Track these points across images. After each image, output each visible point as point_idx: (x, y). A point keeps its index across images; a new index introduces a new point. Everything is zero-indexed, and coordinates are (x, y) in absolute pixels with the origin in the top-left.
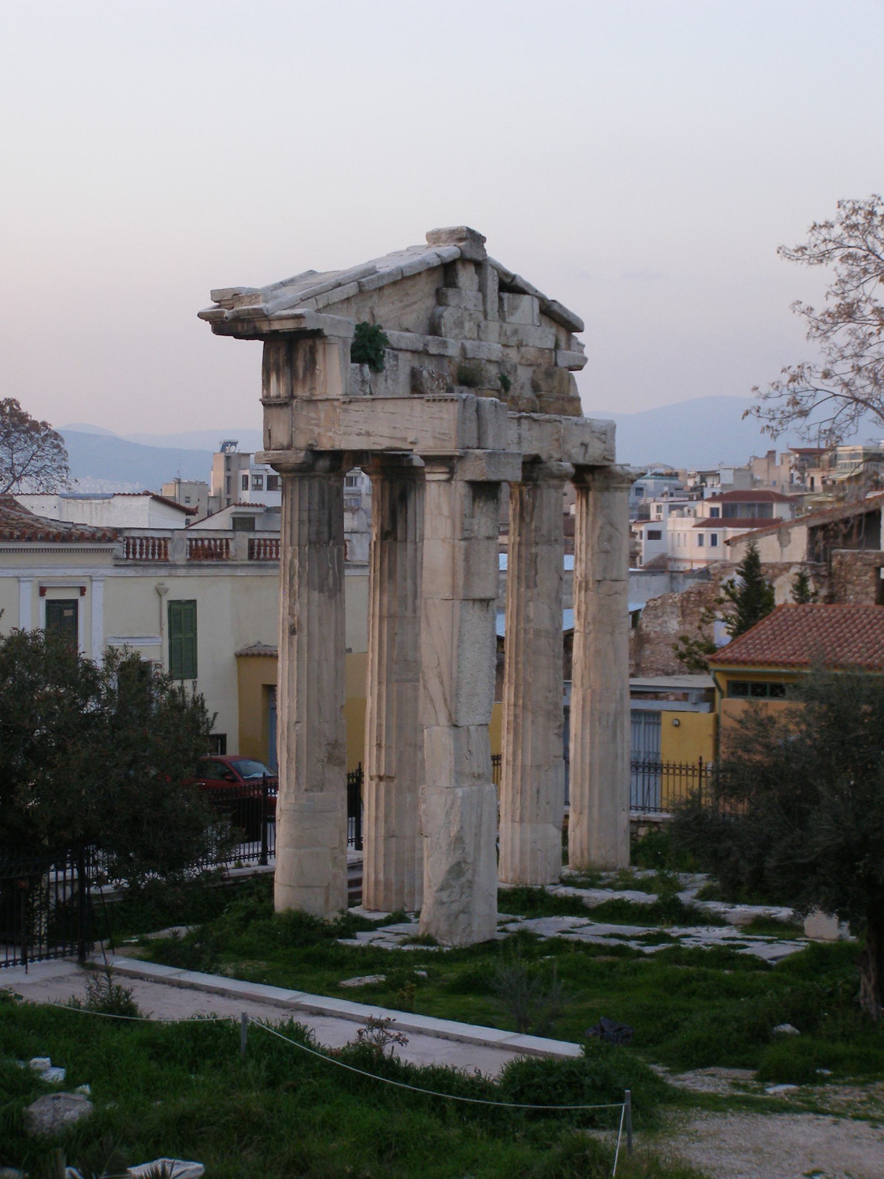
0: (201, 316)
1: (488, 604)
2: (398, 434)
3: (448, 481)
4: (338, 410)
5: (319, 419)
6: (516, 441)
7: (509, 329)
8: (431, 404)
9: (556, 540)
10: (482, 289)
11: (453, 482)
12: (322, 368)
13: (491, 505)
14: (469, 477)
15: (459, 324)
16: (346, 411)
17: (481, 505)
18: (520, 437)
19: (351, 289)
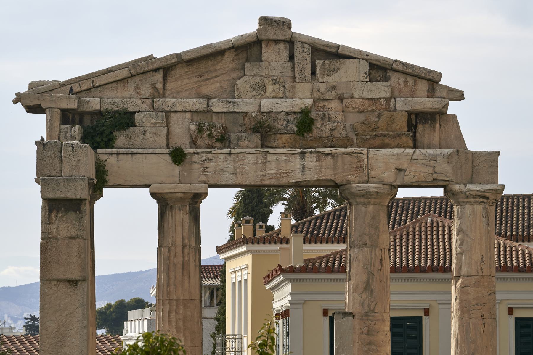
1: (76, 284)
6: (297, 170)
13: (72, 215)
17: (60, 215)
18: (304, 167)
19: (125, 73)
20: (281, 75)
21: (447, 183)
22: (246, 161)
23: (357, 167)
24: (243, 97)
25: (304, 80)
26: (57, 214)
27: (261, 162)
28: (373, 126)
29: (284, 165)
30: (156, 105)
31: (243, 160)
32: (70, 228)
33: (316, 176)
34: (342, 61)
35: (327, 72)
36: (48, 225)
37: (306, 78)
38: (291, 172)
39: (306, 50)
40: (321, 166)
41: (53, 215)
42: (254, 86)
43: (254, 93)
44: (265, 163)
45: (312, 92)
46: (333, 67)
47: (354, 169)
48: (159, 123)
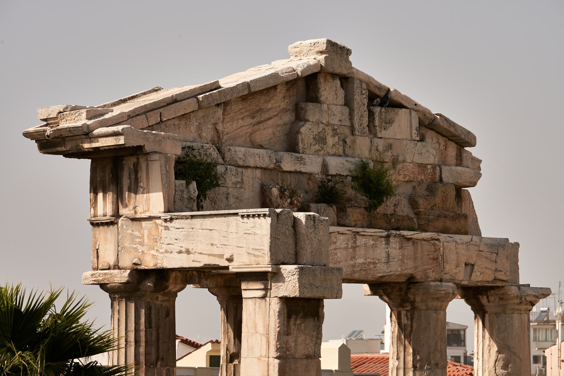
0: (27, 135)
2: (216, 251)
3: (264, 297)
4: (160, 228)
5: (142, 237)
6: (383, 260)
7: (381, 144)
8: (246, 219)
9: (437, 365)
10: (348, 103)
11: (267, 299)
12: (145, 186)
13: (310, 322)
14: (282, 294)
15: (321, 140)
16: (167, 228)
17: (298, 322)
20: (340, 124)
21: (504, 284)
22: (337, 244)
23: (434, 259)
24: (307, 151)
25: (363, 134)
26: (296, 319)
27: (352, 247)
28: (432, 204)
29: (371, 252)
30: (228, 156)
31: (335, 243)
32: (307, 342)
33: (399, 269)
34: (396, 110)
35: (384, 124)
36: (286, 337)
37: (365, 131)
38: (377, 262)
39: (364, 92)
40: (403, 255)
41: (292, 321)
42: (317, 137)
43: (317, 147)
44: (354, 248)
45: (370, 150)
46: (388, 117)
47: (431, 261)
48: (239, 182)
